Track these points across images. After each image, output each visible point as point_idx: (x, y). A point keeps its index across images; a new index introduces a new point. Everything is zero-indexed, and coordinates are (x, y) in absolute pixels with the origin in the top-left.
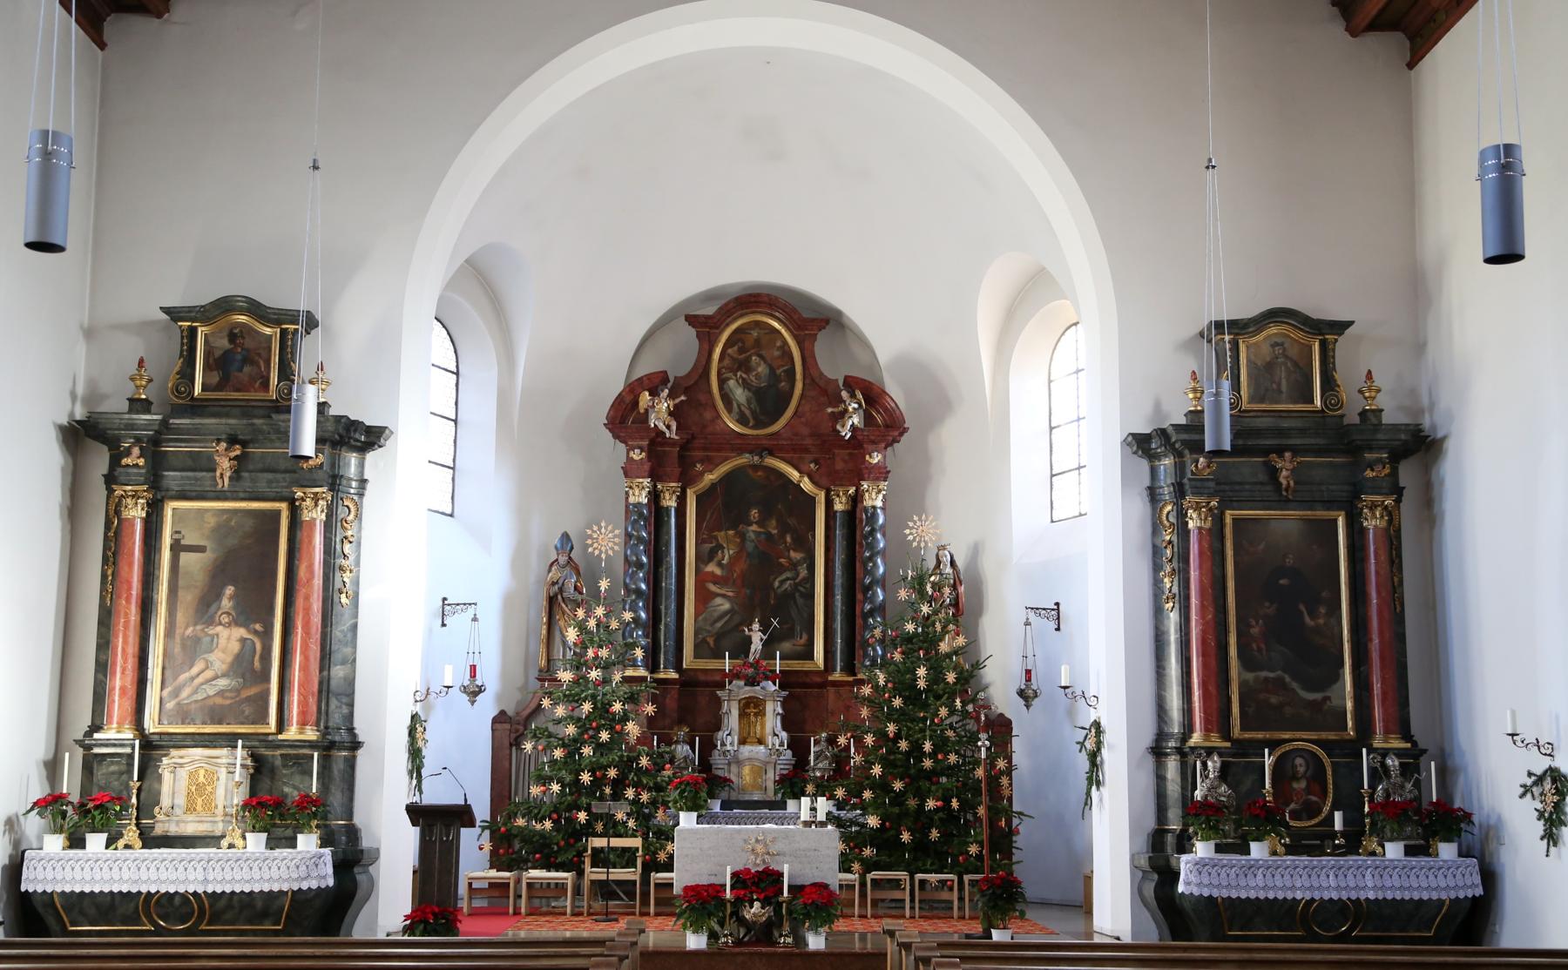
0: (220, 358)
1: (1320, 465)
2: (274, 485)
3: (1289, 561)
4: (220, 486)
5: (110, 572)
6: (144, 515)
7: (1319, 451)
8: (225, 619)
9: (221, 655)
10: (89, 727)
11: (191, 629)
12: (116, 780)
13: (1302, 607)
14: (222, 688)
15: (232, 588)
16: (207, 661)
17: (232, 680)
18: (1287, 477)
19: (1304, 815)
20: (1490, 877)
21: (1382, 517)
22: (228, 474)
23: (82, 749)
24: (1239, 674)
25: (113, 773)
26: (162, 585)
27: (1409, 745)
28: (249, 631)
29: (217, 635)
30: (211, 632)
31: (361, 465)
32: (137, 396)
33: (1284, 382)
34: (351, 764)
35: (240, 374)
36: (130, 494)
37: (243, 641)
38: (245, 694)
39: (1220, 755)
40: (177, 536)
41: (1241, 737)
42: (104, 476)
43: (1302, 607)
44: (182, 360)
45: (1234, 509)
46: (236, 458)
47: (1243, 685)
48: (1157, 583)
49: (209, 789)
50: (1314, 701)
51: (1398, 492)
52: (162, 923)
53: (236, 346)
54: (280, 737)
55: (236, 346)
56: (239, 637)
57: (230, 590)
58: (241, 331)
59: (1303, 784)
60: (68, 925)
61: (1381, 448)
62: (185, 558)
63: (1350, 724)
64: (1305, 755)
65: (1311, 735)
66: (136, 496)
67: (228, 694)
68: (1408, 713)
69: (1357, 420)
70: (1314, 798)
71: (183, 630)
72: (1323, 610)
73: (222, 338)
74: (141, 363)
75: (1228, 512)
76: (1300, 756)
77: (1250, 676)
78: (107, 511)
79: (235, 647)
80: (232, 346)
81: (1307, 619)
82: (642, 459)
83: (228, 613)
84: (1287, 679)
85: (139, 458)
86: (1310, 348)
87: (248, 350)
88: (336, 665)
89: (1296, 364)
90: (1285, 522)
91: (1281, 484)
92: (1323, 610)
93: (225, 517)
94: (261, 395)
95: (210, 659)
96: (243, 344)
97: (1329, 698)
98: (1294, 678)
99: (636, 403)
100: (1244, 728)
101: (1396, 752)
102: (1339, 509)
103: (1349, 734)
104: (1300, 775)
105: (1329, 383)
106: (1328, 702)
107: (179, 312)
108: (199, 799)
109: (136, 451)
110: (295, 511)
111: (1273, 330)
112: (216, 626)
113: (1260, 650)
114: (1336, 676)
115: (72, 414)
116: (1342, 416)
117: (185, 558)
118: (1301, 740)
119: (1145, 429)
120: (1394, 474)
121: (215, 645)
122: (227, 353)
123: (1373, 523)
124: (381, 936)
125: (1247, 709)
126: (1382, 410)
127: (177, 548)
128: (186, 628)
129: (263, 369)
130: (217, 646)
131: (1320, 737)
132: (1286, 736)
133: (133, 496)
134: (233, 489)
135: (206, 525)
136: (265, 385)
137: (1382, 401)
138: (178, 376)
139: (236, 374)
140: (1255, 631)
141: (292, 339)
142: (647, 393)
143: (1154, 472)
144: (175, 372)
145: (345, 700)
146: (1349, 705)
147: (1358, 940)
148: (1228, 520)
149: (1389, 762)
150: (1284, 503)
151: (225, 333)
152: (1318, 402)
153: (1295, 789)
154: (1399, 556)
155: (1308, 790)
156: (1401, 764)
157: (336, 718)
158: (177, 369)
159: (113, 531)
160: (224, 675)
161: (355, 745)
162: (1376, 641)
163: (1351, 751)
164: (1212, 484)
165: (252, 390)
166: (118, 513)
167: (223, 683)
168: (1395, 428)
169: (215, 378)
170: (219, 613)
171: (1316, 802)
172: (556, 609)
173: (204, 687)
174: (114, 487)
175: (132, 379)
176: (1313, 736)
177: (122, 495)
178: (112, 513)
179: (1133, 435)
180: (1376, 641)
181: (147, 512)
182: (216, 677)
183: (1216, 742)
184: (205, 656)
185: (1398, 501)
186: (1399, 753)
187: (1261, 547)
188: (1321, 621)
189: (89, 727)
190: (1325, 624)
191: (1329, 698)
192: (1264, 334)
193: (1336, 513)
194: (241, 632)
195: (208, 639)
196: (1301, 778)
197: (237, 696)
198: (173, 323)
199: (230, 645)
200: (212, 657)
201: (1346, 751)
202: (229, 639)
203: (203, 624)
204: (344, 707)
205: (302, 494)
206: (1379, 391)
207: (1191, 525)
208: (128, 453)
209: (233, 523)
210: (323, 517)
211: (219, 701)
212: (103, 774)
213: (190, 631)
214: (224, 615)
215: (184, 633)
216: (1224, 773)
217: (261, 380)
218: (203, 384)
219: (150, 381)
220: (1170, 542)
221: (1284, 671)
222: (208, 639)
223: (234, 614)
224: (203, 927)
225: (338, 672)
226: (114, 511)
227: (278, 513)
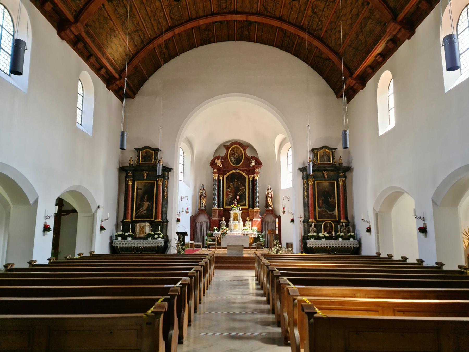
1: (332, 173)
3: (326, 190)
7: (332, 171)
8: (145, 201)
9: (145, 207)
13: (329, 197)
18: (326, 175)
20: (360, 244)
21: (342, 182)
22: (146, 176)
24: (318, 209)
27: (347, 221)
28: (150, 203)
29: (144, 203)
31: (168, 174)
33: (325, 159)
34: (167, 225)
37: (148, 204)
38: (149, 213)
39: (314, 223)
42: (125, 177)
43: (329, 197)
45: (317, 181)
46: (147, 174)
47: (318, 211)
48: (304, 193)
51: (346, 177)
52: (136, 252)
54: (155, 221)
56: (148, 204)
57: (146, 196)
59: (329, 228)
61: (342, 170)
62: (138, 190)
63: (337, 217)
66: (130, 180)
69: (338, 165)
70: (331, 230)
72: (332, 198)
75: (316, 181)
77: (319, 209)
79: (147, 205)
81: (330, 200)
83: (146, 200)
84: (326, 210)
86: (330, 153)
89: (327, 155)
90: (326, 183)
91: (325, 176)
92: (332, 198)
94: (151, 163)
98: (327, 210)
99: (215, 161)
100: (319, 218)
102: (335, 180)
105: (333, 159)
109: (130, 173)
110: (157, 183)
111: (323, 150)
113: (321, 205)
114: (334, 209)
115: (119, 166)
116: (336, 164)
117: (138, 190)
118: (329, 220)
119: (301, 167)
120: (345, 174)
122: (145, 155)
123: (341, 183)
124: (172, 254)
126: (342, 163)
127: (137, 189)
132: (326, 220)
137: (343, 162)
140: (320, 202)
143: (303, 174)
146: (337, 214)
147: (337, 254)
148: (316, 183)
149: (343, 224)
150: (325, 180)
152: (331, 162)
154: (346, 188)
155: (330, 229)
156: (346, 225)
157: (164, 217)
160: (146, 210)
161: (167, 222)
162: (341, 203)
163: (339, 222)
164: (313, 176)
166: (127, 183)
167: (145, 211)
168: (344, 166)
169: (143, 160)
172: (201, 197)
174: (127, 179)
175: (130, 160)
176: (331, 220)
178: (126, 183)
179: (299, 168)
180: (341, 203)
182: (144, 211)
183: (313, 221)
185: (346, 179)
186: (345, 223)
187: (321, 187)
188: (332, 200)
190: (333, 200)
191: (333, 213)
192: (322, 150)
193: (334, 181)
194: (148, 203)
198: (136, 151)
199: (146, 205)
202: (146, 204)
206: (342, 160)
207: (309, 183)
208: (129, 173)
210: (162, 183)
211: (145, 215)
216: (315, 226)
219: (133, 161)
220: (306, 186)
221: (326, 208)
224: (143, 253)
225: (164, 209)
226: (127, 183)
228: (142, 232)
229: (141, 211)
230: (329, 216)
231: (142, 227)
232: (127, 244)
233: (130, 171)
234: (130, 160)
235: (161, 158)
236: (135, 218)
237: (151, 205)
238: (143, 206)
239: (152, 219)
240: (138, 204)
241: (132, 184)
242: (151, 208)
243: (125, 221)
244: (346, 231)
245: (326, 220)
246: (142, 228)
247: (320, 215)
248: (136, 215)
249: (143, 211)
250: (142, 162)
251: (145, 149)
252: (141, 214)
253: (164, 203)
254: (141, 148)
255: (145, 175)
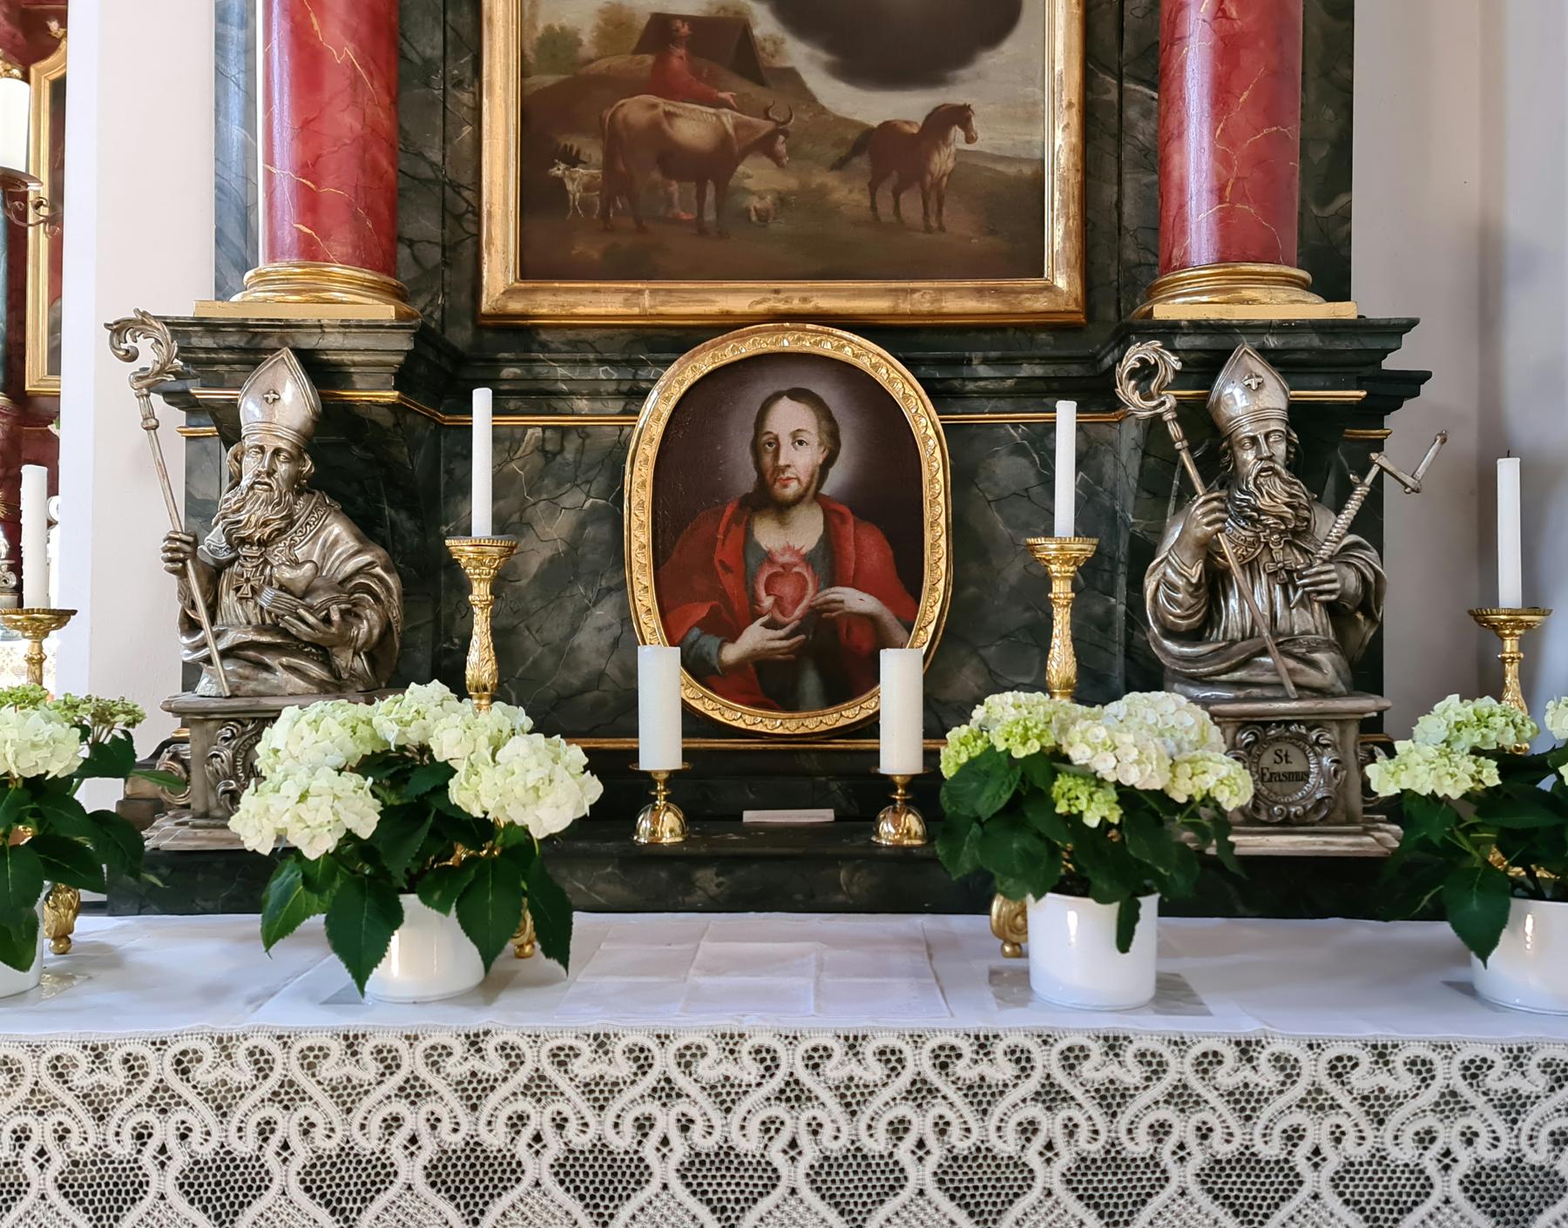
19: (811, 682)
41: (515, 306)
50: (887, 126)
59: (806, 531)
63: (1058, 234)
64: (823, 390)
65: (861, 294)
68: (1345, 217)
76: (797, 395)
97: (960, 116)
101: (1272, 342)
103: (1051, 288)
104: (793, 489)
106: (957, 133)
125: (559, 170)
131: (905, 306)
153: (768, 557)
156: (1298, 414)
171: (871, 619)
176: (871, 300)
191: (960, 116)
196: (798, 500)
201: (1026, 370)
230: (848, 193)
244: (1308, 621)
245: (738, 300)
247: (576, 180)
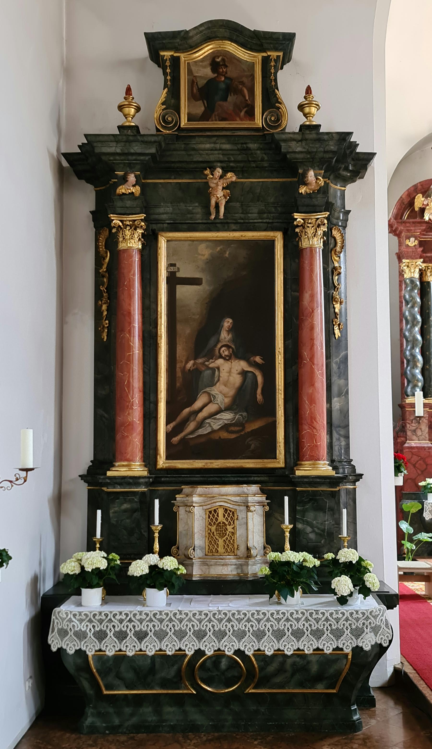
0: (202, 87)
2: (265, 215)
4: (213, 217)
5: (104, 307)
6: (140, 247)
8: (225, 352)
9: (222, 388)
10: (91, 461)
11: (192, 362)
12: (127, 518)
14: (226, 422)
15: (231, 321)
16: (209, 394)
17: (236, 414)
23: (87, 485)
25: (125, 511)
26: (161, 318)
29: (218, 368)
30: (211, 365)
32: (127, 124)
35: (224, 104)
36: (128, 223)
37: (244, 373)
40: (172, 269)
44: (166, 90)
49: (230, 528)
53: (219, 74)
55: (219, 74)
56: (240, 369)
57: (227, 323)
58: (223, 60)
60: (103, 689)
67: (232, 428)
71: (183, 365)
73: (205, 67)
74: (128, 91)
78: (97, 247)
79: (237, 380)
80: (216, 75)
82: (415, 245)
85: (134, 186)
87: (230, 79)
88: (334, 398)
93: (219, 249)
94: (246, 124)
95: (213, 393)
96: (226, 73)
99: (411, 204)
107: (164, 38)
108: (220, 540)
109: (132, 178)
112: (216, 359)
121: (216, 379)
122: (211, 82)
128: (187, 362)
129: (247, 98)
130: (219, 380)
133: (131, 226)
134: (225, 221)
135: (200, 257)
136: (251, 114)
138: (164, 106)
139: (221, 103)
141: (274, 66)
142: (420, 195)
144: (160, 102)
145: (342, 432)
151: (208, 62)
158: (162, 98)
159: (105, 266)
160: (228, 409)
165: (238, 119)
167: (227, 416)
170: (219, 346)
173: (208, 421)
175: (121, 108)
177: (119, 226)
178: (102, 249)
181: (143, 244)
184: (208, 389)
189: (91, 461)
194: (242, 365)
195: (209, 372)
197: (241, 431)
200: (215, 390)
202: (230, 372)
203: (204, 357)
204: (342, 439)
205: (302, 221)
208: (124, 180)
209: (227, 255)
211: (224, 435)
212: (115, 512)
213: (190, 364)
214: (223, 349)
215: (185, 367)
217: (245, 109)
218: (188, 114)
222: (209, 372)
223: (233, 346)
225: (336, 403)
227: (271, 243)
228: (221, 542)
229: (201, 415)
231: (221, 512)
232: (146, 634)
233: (131, 167)
234: (121, 108)
235: (308, 90)
236: (168, 457)
237: (260, 379)
238: (212, 384)
239: (270, 464)
240: (179, 374)
241: (141, 252)
242: (259, 397)
243: (111, 478)
246: (221, 518)
248: (175, 440)
249: (212, 415)
250: (190, 118)
251: (208, 39)
252: (201, 432)
253: (335, 361)
254: (187, 32)
255: (220, 193)
